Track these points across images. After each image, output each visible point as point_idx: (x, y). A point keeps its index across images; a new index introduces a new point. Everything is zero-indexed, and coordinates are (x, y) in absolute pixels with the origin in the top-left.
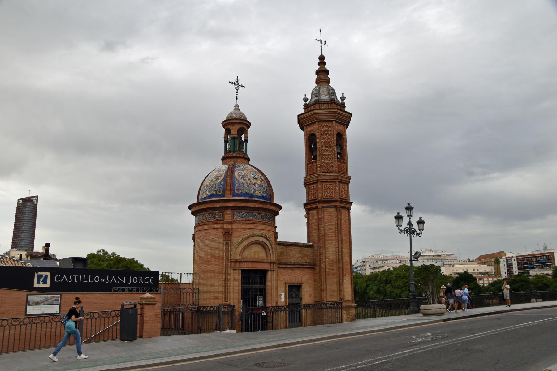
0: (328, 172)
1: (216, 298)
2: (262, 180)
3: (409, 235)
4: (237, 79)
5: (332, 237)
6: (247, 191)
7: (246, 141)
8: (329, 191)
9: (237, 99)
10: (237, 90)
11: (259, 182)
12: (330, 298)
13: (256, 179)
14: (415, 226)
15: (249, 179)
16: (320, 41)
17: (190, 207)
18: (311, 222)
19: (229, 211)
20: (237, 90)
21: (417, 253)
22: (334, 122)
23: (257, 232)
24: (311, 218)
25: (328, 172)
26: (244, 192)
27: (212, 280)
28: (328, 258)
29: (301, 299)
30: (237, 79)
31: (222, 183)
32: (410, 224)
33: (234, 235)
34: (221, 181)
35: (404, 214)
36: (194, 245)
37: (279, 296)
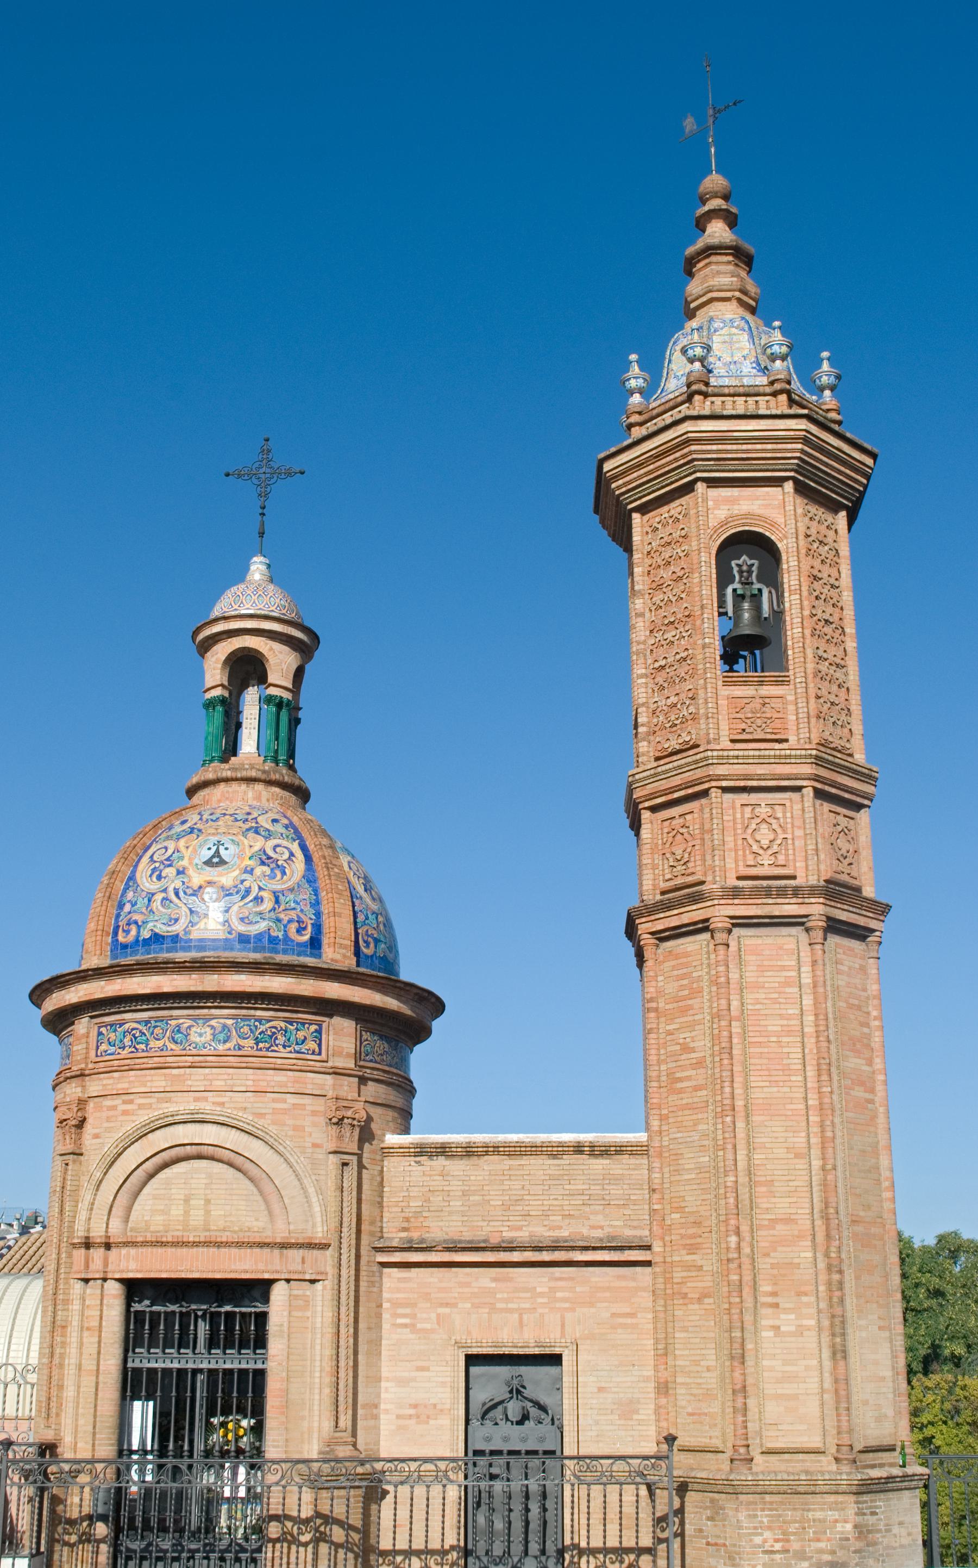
5: (697, 1088)
6: (161, 929)
8: (679, 852)
13: (222, 862)
22: (700, 487)
23: (182, 1105)
26: (146, 934)
28: (680, 1209)
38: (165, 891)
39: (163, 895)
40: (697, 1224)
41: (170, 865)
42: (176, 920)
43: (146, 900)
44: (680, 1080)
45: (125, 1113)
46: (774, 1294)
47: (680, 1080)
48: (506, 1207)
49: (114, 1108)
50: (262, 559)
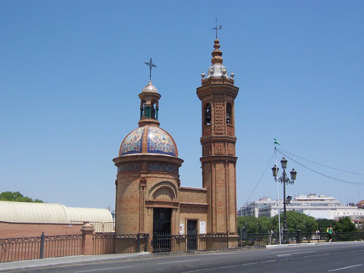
0: (219, 134)
1: (135, 229)
2: (170, 140)
3: (283, 183)
4: (151, 61)
5: (222, 184)
6: (159, 149)
7: (157, 109)
9: (150, 76)
10: (151, 69)
11: (167, 142)
12: (219, 231)
13: (165, 139)
14: (289, 176)
15: (160, 140)
16: (216, 28)
17: (114, 160)
18: (205, 172)
19: (145, 164)
20: (151, 69)
21: (289, 197)
24: (205, 169)
25: (219, 134)
26: (156, 150)
27: (132, 215)
28: (218, 200)
29: (197, 231)
30: (151, 61)
31: (140, 142)
32: (284, 174)
33: (147, 182)
34: (139, 141)
35: (279, 165)
36: (116, 189)
37: (180, 228)
38: (158, 143)
39: (158, 144)
40: (222, 202)
41: (157, 138)
42: (161, 148)
43: (155, 144)
44: (219, 182)
45: (156, 180)
46: (231, 212)
47: (219, 182)
48: (191, 198)
49: (154, 179)
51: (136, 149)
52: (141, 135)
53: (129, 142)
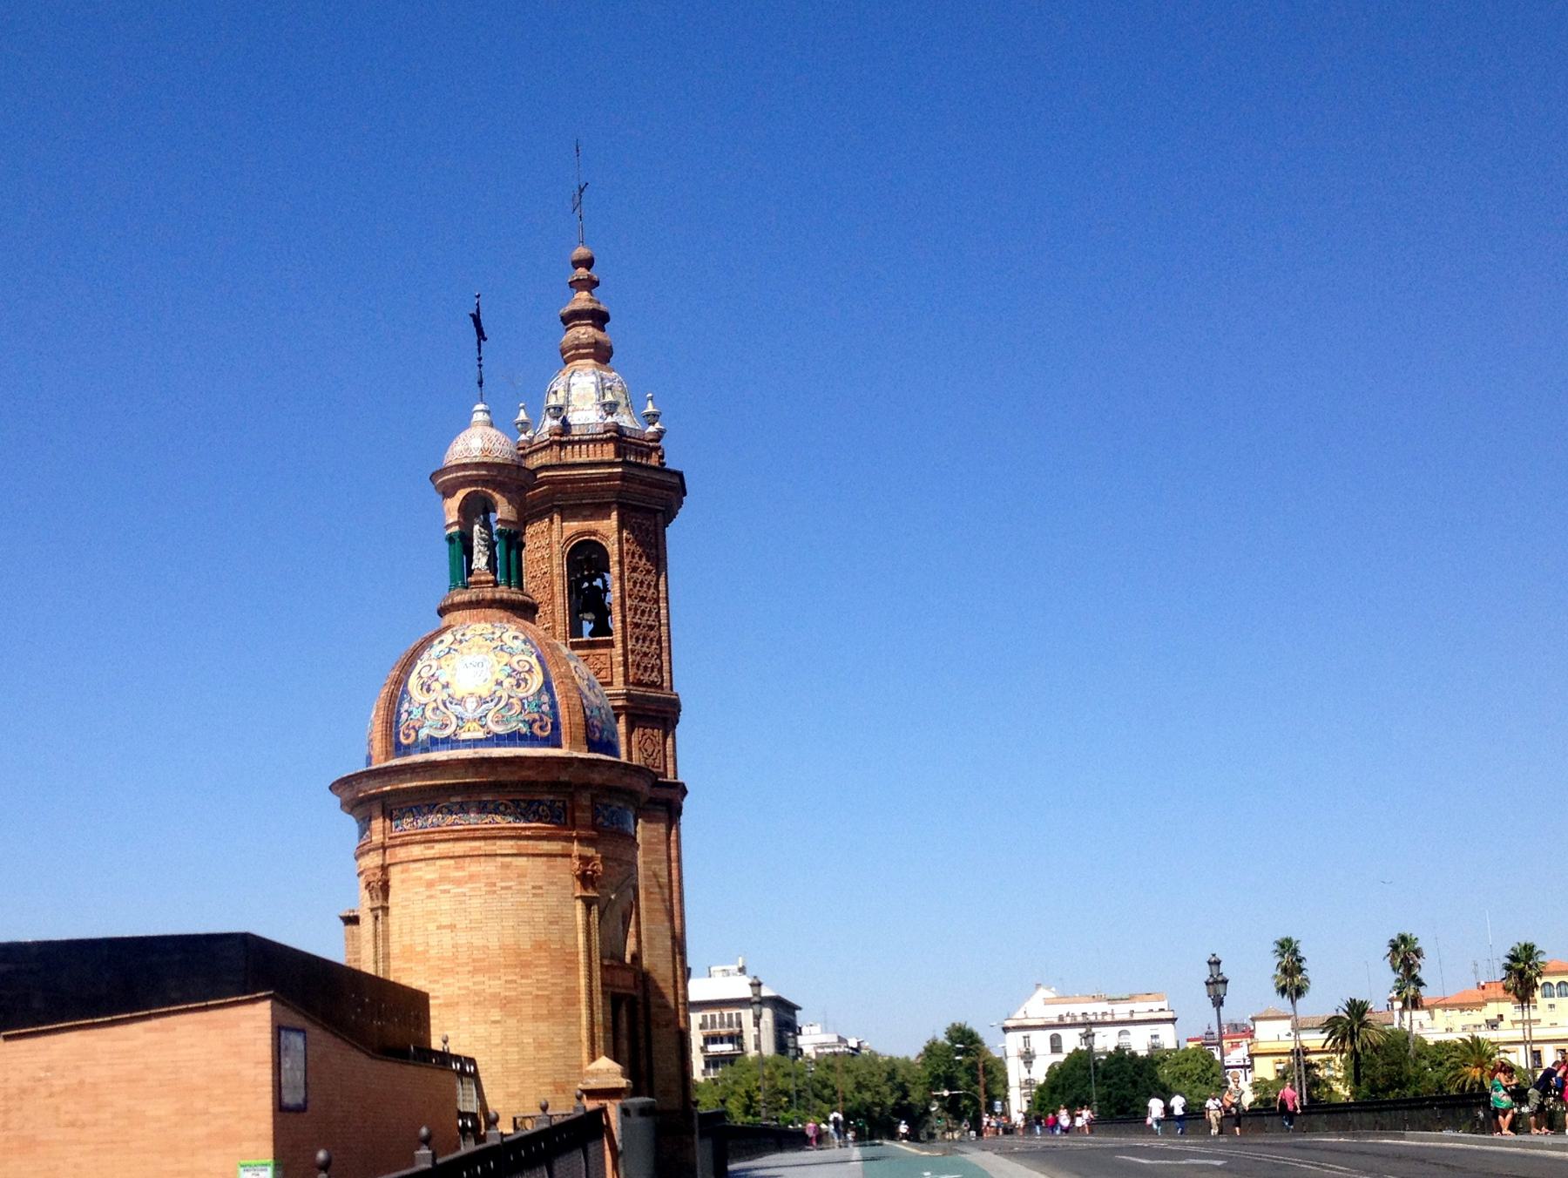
0: (646, 685)
9: (480, 383)
34: (539, 691)
50: (480, 406)
51: (536, 726)
52: (534, 660)
53: (485, 694)
